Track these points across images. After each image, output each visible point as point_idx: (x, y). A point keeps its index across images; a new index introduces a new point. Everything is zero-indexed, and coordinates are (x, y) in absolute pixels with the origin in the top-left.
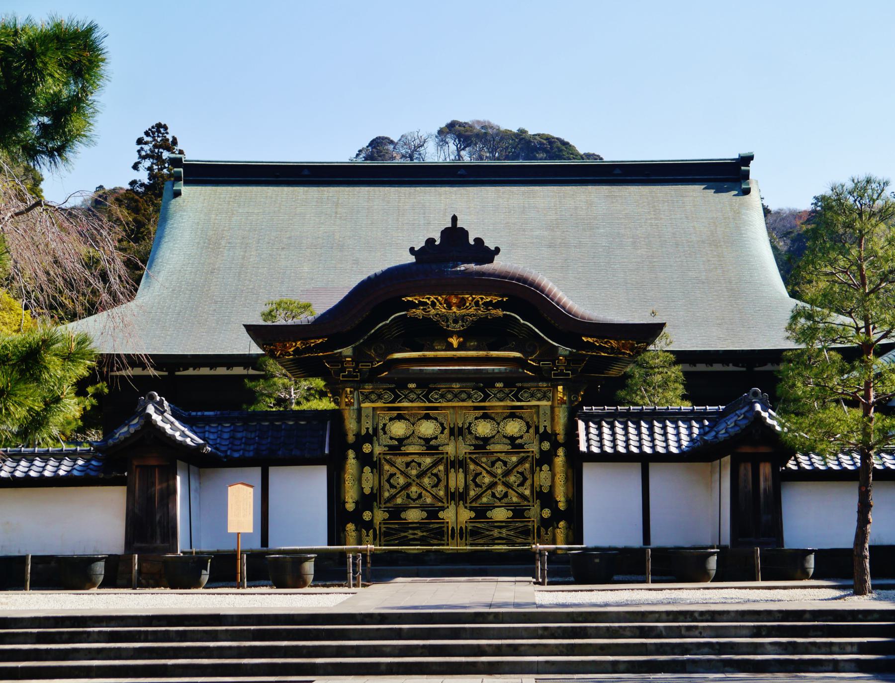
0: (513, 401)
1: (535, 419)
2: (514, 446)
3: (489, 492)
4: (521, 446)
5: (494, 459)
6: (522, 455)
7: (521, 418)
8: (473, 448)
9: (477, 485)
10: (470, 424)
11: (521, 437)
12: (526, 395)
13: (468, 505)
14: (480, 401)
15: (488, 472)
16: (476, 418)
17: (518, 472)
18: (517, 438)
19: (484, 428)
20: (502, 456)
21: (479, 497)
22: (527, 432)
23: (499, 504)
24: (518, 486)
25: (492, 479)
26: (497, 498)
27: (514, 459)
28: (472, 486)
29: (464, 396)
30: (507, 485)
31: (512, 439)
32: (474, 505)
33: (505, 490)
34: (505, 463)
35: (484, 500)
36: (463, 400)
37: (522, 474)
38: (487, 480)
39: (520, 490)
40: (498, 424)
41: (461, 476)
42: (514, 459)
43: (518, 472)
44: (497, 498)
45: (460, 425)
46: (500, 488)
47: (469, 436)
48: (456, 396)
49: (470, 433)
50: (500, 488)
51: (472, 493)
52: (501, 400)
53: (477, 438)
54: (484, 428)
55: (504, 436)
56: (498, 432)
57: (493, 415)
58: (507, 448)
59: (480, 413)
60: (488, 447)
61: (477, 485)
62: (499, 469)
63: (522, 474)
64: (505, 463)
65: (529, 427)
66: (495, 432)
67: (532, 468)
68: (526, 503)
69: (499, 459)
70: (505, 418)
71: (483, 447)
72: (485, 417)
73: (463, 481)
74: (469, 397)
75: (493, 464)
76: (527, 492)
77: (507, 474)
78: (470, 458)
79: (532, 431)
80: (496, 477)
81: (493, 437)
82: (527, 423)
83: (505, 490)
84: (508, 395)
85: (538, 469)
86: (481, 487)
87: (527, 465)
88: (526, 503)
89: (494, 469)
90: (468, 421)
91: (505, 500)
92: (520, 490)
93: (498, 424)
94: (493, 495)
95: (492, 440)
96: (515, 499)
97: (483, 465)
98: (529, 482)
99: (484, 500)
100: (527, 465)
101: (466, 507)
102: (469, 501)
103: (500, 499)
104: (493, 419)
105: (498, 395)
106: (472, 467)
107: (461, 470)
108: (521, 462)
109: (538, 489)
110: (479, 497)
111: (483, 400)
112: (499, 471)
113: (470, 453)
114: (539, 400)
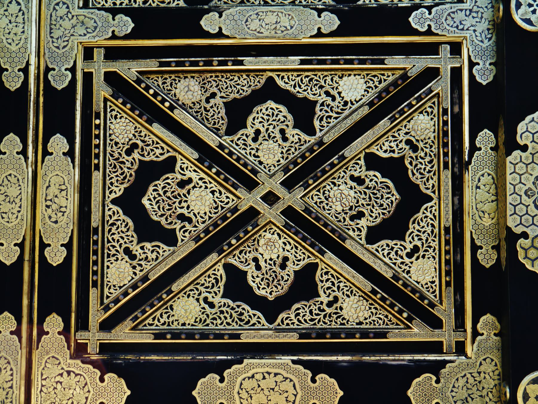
3: (213, 265)
5: (245, 87)
6: (396, 62)
8: (126, 24)
9: (149, 230)
13: (93, 338)
15: (207, 155)
17: (373, 162)
20: (285, 70)
21: (152, 292)
23: (267, 336)
24: (374, 235)
25: (228, 199)
26: (258, 303)
27: (354, 88)
28: (121, 229)
30: (304, 225)
32: (124, 334)
33: (300, 256)
34: (303, 113)
35: (186, 311)
37: (393, 169)
38: (204, 201)
39: (383, 257)
41: (61, 173)
42: (354, 88)
43: (373, 162)
44: (258, 303)
46: (272, 252)
50: (272, 252)
51: (119, 274)
60: (209, 22)
61: (149, 230)
62: (270, 144)
63: (393, 169)
64: (303, 113)
67: (451, 134)
68: (419, 332)
69: (270, 91)
73: (71, 203)
75: (238, 113)
76: (424, 273)
77: (305, 171)
78: (111, 78)
80: (251, 185)
83: (300, 256)
85: (486, 138)
86: (170, 238)
87: (423, 125)
88: (419, 332)
89: (237, 145)
91: (299, 316)
92: (383, 257)
94: (237, 286)
96: (355, 310)
97: (179, 115)
98: (427, 222)
99: (186, 311)
100: (423, 125)
101: (80, 352)
102: (96, 316)
103: (271, 309)
106: (123, 127)
107: (58, 143)
108: (390, 103)
109: (487, 258)
110: (152, 292)
112: (271, 154)
113: (112, 54)
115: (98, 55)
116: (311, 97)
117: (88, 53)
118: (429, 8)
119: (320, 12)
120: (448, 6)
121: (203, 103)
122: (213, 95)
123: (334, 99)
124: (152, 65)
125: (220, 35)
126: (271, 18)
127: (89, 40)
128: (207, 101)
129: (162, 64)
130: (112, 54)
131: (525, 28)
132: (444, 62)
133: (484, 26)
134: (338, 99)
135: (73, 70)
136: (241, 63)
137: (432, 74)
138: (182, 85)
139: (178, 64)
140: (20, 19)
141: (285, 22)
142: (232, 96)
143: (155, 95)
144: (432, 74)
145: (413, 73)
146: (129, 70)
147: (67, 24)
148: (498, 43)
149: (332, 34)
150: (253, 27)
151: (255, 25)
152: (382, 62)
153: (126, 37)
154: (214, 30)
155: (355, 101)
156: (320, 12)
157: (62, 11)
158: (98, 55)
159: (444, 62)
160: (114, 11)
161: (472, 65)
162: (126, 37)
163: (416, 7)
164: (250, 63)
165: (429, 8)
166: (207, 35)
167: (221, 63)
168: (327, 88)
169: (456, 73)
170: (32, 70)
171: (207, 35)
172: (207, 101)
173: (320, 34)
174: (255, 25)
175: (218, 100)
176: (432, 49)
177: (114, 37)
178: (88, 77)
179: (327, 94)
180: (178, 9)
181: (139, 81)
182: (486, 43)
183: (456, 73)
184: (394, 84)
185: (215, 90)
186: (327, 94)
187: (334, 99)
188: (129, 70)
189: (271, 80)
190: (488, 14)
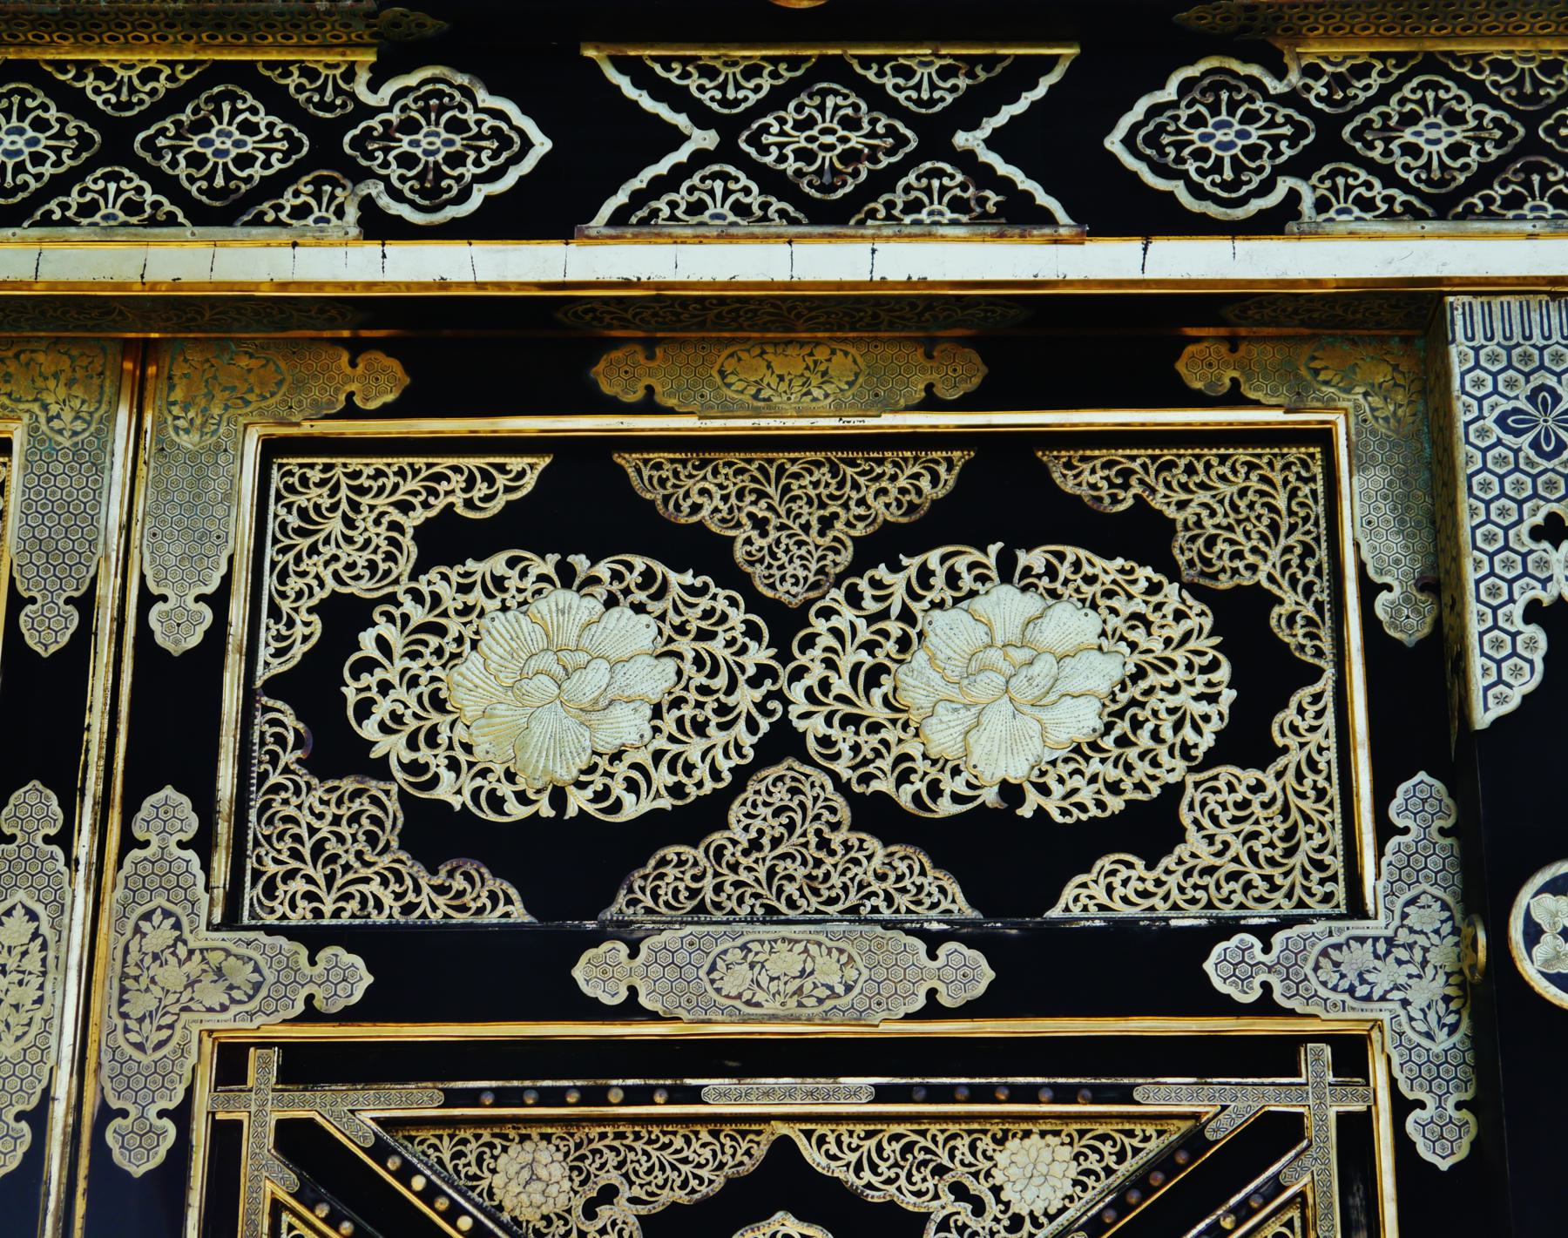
0: (1019, 216)
1: (1370, 530)
2: (1038, 967)
4: (1161, 964)
7: (1142, 537)
8: (352, 976)
10: (346, 617)
11: (1150, 828)
12: (1224, 136)
14: (497, 223)
16: (447, 541)
18: (1081, 844)
19: (558, 686)
22: (1246, 742)
29: (236, 140)
31: (1001, 853)
36: (225, 209)
40: (785, 625)
45: (179, 631)
47: (312, 804)
48: (114, 142)
49: (337, 751)
52: (830, 214)
53: (435, 833)
54: (558, 686)
55: (876, 816)
56: (782, 743)
57: (703, 497)
58: (911, 972)
59: (507, 452)
60: (599, 973)
65: (1264, 671)
66: (713, 754)
70: (882, 547)
71: (530, 971)
72: (587, 515)
74: (328, 151)
78: (301, 1143)
79: (1301, 726)
81: (698, 819)
82: (1241, 618)
84: (935, 135)
90: (320, 577)
93: (785, 625)
95: (679, 865)
104: (705, 553)
105: (781, 142)
111: (541, 211)
113: (304, 1066)
114: (1443, 203)
115: (261, 1069)
116: (909, 1203)
117: (231, 1063)
118: (1265, 934)
119: (933, 942)
120: (1320, 926)
121: (577, 1220)
122: (608, 1194)
123: (979, 1209)
124: (422, 1100)
125: (631, 1009)
126: (787, 962)
127: (234, 1025)
128: (590, 1212)
129: (452, 1099)
130: (304, 1066)
131: (1556, 1002)
132: (1315, 1096)
133: (1430, 988)
134: (993, 1209)
135: (182, 1116)
136: (695, 1096)
137: (1279, 1132)
138: (511, 1161)
139: (502, 1098)
140: (33, 963)
141: (828, 971)
142: (666, 1197)
143: (430, 1193)
144: (1279, 1132)
145: (1221, 1131)
146: (353, 1115)
147: (172, 975)
148: (1477, 1041)
149: (970, 1010)
150: (730, 987)
151: (736, 980)
152: (1125, 1095)
153: (349, 1015)
154: (613, 997)
155: (1046, 1214)
156: (933, 942)
157: (159, 935)
158: (261, 1069)
159: (1315, 1096)
160: (314, 938)
161: (1402, 1107)
162: (349, 1015)
163: (1225, 929)
164: (722, 1095)
165: (1265, 934)
166: (594, 1010)
167: (632, 1097)
168: (959, 1173)
169: (1355, 1131)
170: (59, 1112)
171: (594, 1010)
172: (590, 1212)
173: (932, 1009)
174: (736, 980)
175: (621, 1211)
176: (1277, 1057)
177: (311, 1014)
178: (226, 1136)
179: (959, 1191)
180: (509, 931)
181: (380, 1151)
182: (1443, 1042)
183: (1355, 1131)
184: (1165, 1163)
185: (614, 1178)
186: (959, 1191)
187: (979, 1209)
188: (353, 1115)
189: (784, 1146)
190: (1443, 953)
